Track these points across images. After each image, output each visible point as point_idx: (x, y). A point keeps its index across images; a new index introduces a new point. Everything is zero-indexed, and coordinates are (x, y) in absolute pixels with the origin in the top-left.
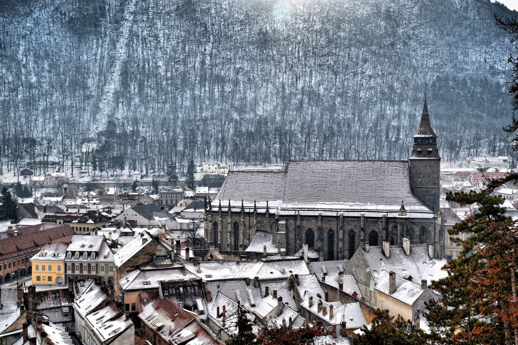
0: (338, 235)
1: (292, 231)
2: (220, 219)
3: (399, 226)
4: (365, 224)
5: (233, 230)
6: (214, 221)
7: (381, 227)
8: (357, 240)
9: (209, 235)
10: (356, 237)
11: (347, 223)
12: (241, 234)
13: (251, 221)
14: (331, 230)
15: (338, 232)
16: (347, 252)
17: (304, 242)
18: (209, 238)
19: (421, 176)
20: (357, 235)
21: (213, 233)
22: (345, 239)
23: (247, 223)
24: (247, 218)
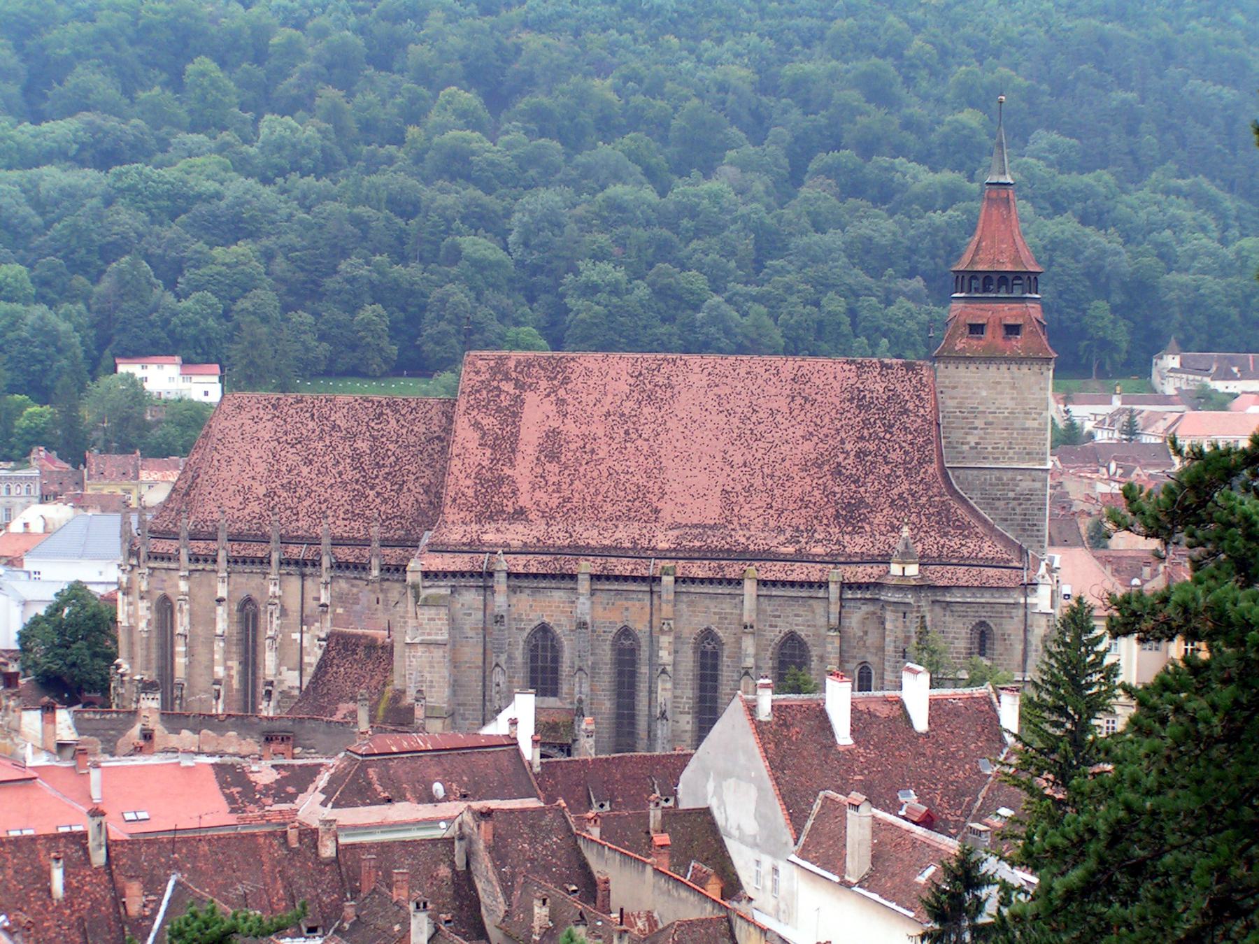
0: (653, 653)
2: (183, 586)
3: (889, 616)
4: (759, 611)
5: (235, 629)
7: (822, 621)
8: (726, 673)
9: (139, 651)
10: (725, 660)
13: (310, 594)
14: (626, 632)
15: (653, 641)
16: (689, 718)
17: (521, 675)
18: (139, 660)
20: (726, 652)
21: (154, 641)
23: (293, 604)
24: (294, 584)
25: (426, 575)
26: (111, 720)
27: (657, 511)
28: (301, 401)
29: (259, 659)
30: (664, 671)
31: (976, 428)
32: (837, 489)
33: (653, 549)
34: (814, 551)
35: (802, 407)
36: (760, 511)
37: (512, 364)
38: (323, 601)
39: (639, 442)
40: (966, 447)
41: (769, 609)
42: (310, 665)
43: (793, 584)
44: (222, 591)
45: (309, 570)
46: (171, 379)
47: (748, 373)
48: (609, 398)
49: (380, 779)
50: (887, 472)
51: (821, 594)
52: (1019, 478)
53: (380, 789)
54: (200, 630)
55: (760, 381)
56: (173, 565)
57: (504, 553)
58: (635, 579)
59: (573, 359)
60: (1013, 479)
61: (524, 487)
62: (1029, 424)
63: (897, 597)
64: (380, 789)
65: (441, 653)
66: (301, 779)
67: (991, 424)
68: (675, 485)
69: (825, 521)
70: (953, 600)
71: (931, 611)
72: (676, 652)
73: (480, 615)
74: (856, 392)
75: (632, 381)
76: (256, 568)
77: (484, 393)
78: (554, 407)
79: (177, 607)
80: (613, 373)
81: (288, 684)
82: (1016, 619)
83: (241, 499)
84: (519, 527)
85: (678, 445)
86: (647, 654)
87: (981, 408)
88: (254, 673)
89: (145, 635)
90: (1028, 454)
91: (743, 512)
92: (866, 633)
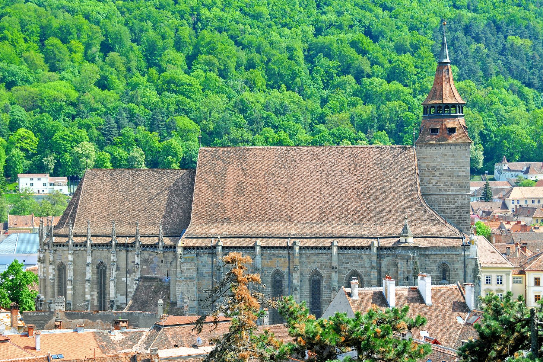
1: (206, 275)
2: (70, 258)
3: (399, 261)
4: (339, 261)
5: (95, 277)
6: (58, 262)
7: (367, 265)
8: (324, 290)
10: (324, 284)
11: (307, 258)
12: (111, 283)
13: (130, 260)
14: (278, 272)
18: (49, 293)
19: (437, 174)
20: (324, 280)
21: (56, 284)
22: (304, 288)
23: (123, 265)
24: (123, 254)
25: (185, 248)
26: (40, 316)
27: (290, 217)
28: (124, 172)
29: (107, 291)
30: (296, 290)
31: (435, 176)
32: (372, 205)
33: (289, 234)
34: (363, 233)
35: (355, 168)
36: (337, 216)
37: (221, 152)
38: (136, 262)
39: (280, 186)
40: (431, 185)
41: (343, 260)
42: (131, 292)
43: (354, 248)
44: (89, 260)
45: (129, 248)
46: (44, 185)
47: (329, 154)
48: (266, 167)
49: (171, 336)
50: (396, 196)
51: (367, 252)
52: (456, 199)
53: (171, 341)
54: (78, 278)
55: (335, 157)
56: (65, 248)
57: (221, 238)
58: (281, 248)
59: (248, 149)
60: (454, 199)
61: (228, 207)
62: (461, 173)
63: (404, 253)
64: (171, 341)
65: (193, 284)
66: (134, 339)
67: (443, 174)
68: (298, 205)
69: (368, 219)
70: (430, 253)
71: (420, 259)
72: (301, 281)
73: (210, 266)
74: (380, 161)
75: (276, 159)
76: (105, 249)
77: (209, 166)
78: (240, 171)
79: (67, 268)
80: (267, 155)
81: (120, 302)
82: (460, 262)
83: (96, 217)
84: (227, 225)
85: (298, 187)
86: (288, 282)
87: (438, 167)
88: (104, 298)
89: (52, 282)
90: (460, 187)
91: (329, 216)
92: (389, 270)
